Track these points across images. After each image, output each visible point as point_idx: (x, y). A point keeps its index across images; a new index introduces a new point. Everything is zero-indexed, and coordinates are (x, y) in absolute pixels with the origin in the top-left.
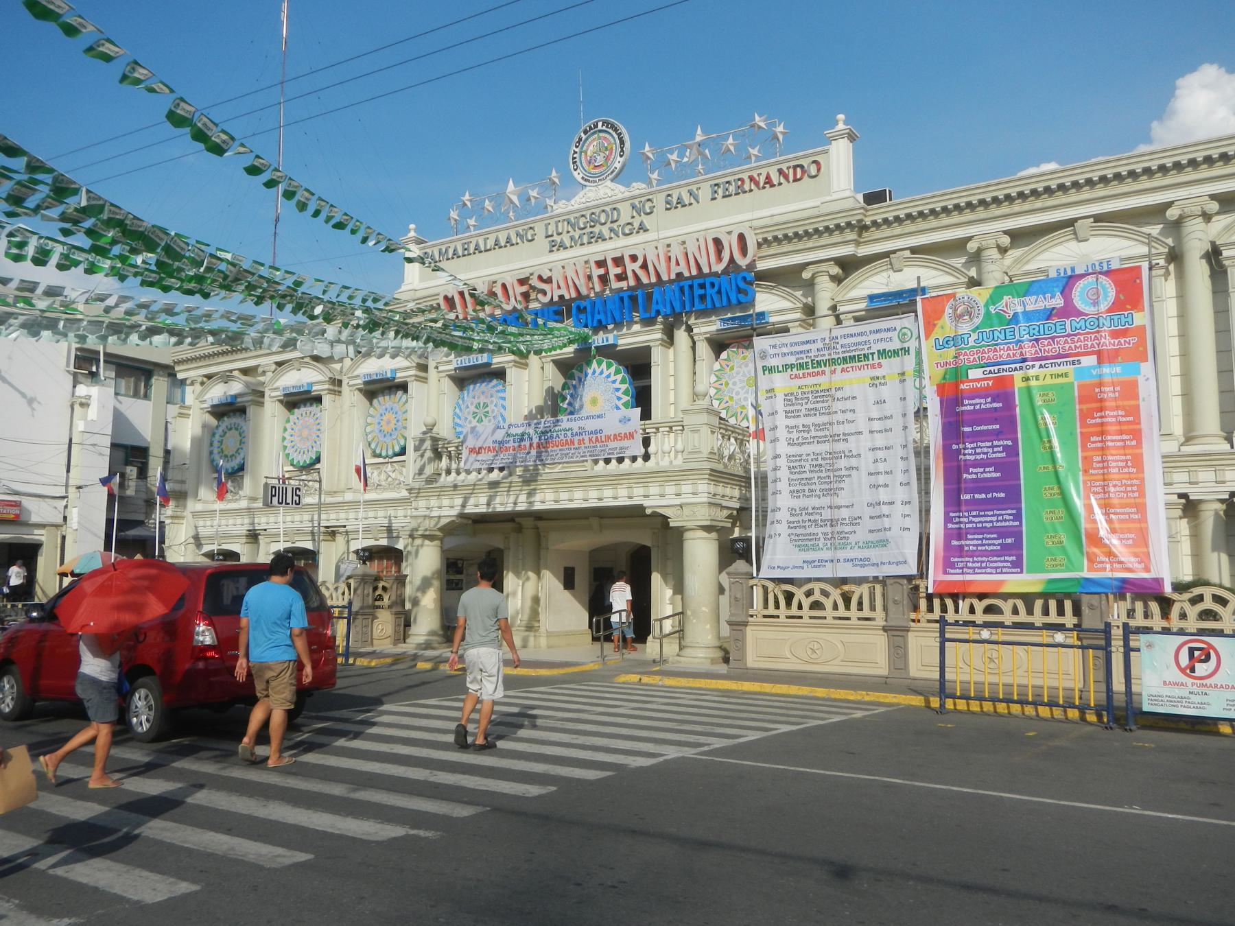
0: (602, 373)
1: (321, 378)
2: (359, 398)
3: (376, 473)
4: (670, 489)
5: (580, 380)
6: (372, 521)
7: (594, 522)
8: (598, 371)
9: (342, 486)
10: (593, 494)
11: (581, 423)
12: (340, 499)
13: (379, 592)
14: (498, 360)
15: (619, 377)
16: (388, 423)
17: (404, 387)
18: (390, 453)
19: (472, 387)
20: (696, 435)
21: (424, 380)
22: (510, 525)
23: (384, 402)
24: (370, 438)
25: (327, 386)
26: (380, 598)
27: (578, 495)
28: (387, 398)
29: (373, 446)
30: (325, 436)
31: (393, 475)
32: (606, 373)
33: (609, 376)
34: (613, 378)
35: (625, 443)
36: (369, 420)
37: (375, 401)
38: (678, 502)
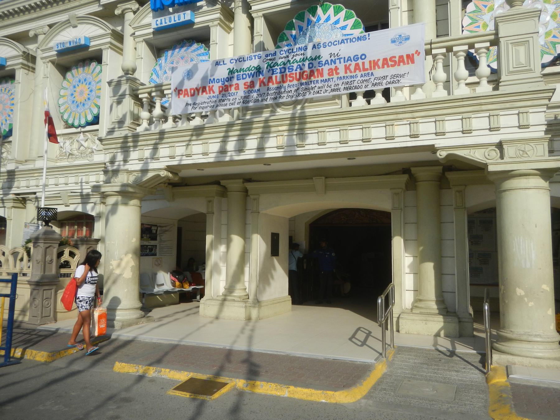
0: (328, 19)
1: (14, 53)
2: (51, 70)
3: (68, 142)
4: (479, 122)
5: (301, 29)
6: (62, 187)
7: (319, 182)
8: (323, 17)
9: (34, 155)
10: (355, 134)
11: (334, 49)
12: (30, 166)
13: (66, 256)
14: (200, 20)
15: (351, 22)
16: (82, 93)
17: (97, 58)
18: (83, 122)
19: (170, 52)
20: (522, 49)
21: (120, 51)
22: (215, 188)
23: (78, 74)
24: (62, 109)
25: (21, 61)
26: (66, 265)
27: (332, 136)
28: (81, 70)
29: (62, 109)
30: (18, 108)
31: (86, 144)
32: (333, 19)
33: (337, 22)
34: (342, 24)
35: (402, 69)
36: (62, 92)
37: (69, 75)
38: (495, 138)
